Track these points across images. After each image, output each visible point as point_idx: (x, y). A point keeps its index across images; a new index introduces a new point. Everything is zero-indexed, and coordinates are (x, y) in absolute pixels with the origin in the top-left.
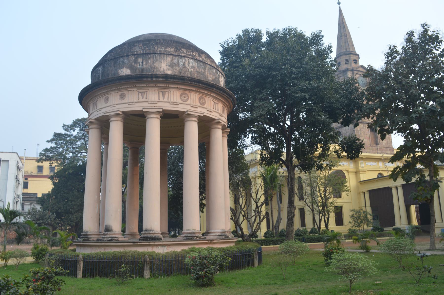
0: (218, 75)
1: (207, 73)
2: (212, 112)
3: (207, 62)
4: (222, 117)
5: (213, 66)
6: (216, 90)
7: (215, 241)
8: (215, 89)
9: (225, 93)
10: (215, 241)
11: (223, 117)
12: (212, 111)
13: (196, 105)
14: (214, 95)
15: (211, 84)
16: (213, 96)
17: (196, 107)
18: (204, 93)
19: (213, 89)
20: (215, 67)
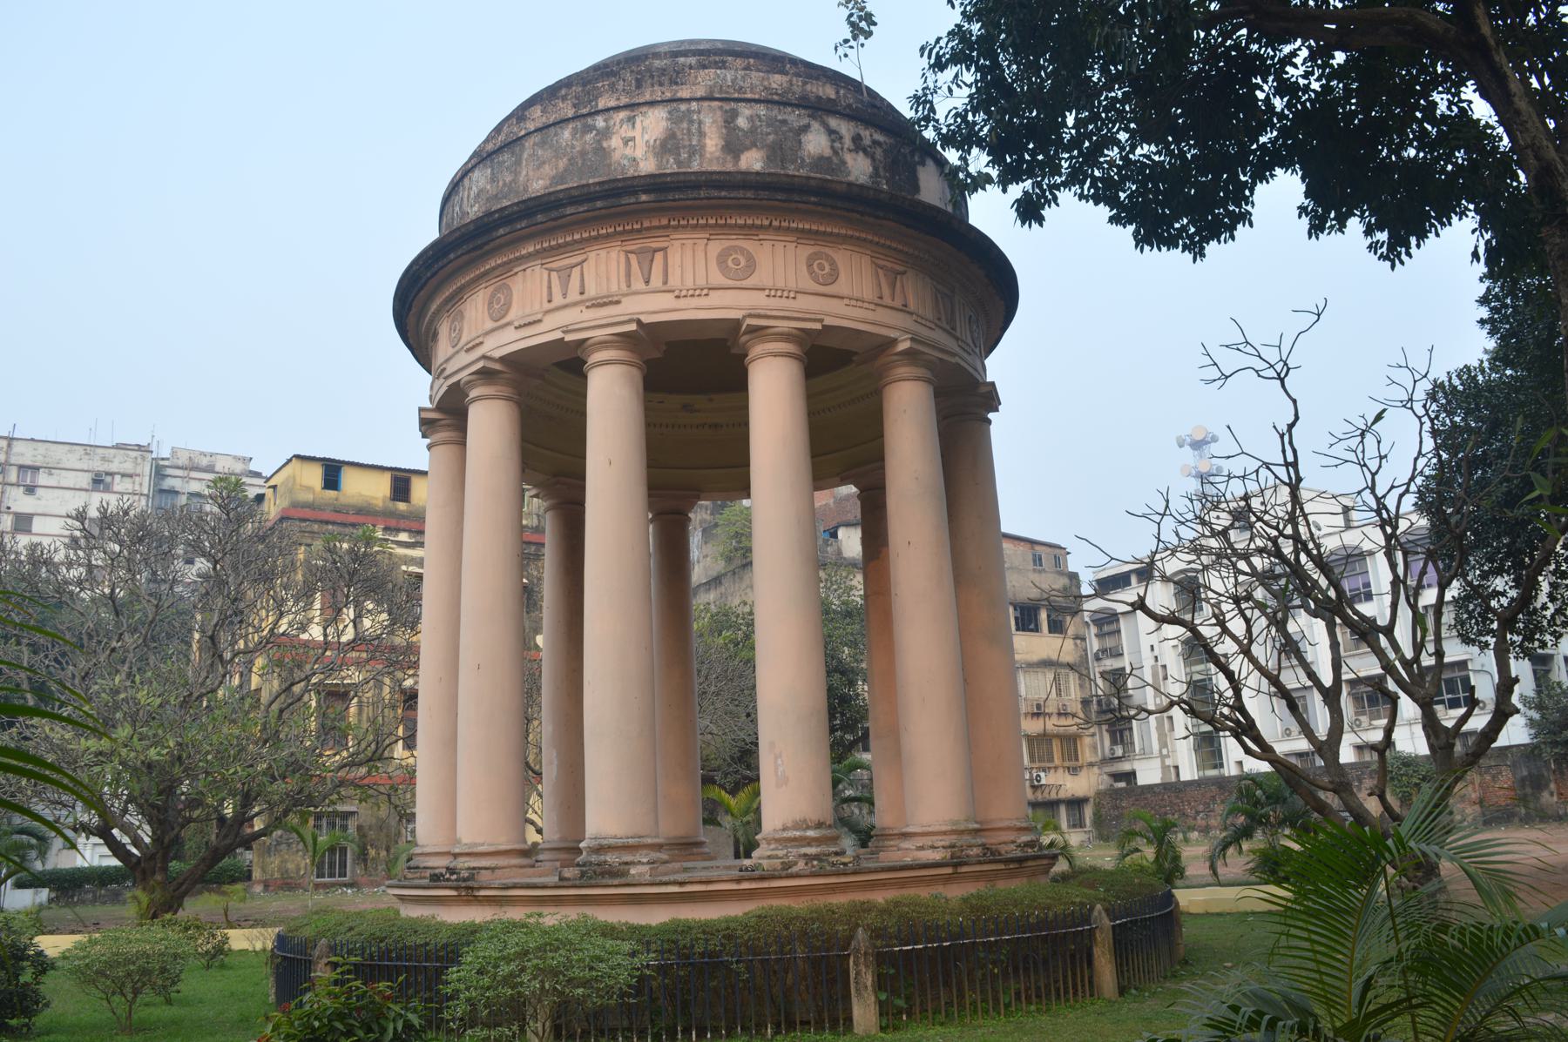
0: (589, 137)
1: (524, 173)
2: (540, 321)
3: (523, 133)
4: (618, 302)
5: (554, 124)
6: (507, 229)
7: (483, 893)
8: (501, 231)
9: (564, 206)
10: (483, 893)
11: (624, 300)
12: (539, 317)
13: (480, 332)
14: (530, 248)
15: (472, 227)
16: (530, 255)
17: (477, 341)
18: (494, 269)
19: (495, 234)
20: (570, 113)
